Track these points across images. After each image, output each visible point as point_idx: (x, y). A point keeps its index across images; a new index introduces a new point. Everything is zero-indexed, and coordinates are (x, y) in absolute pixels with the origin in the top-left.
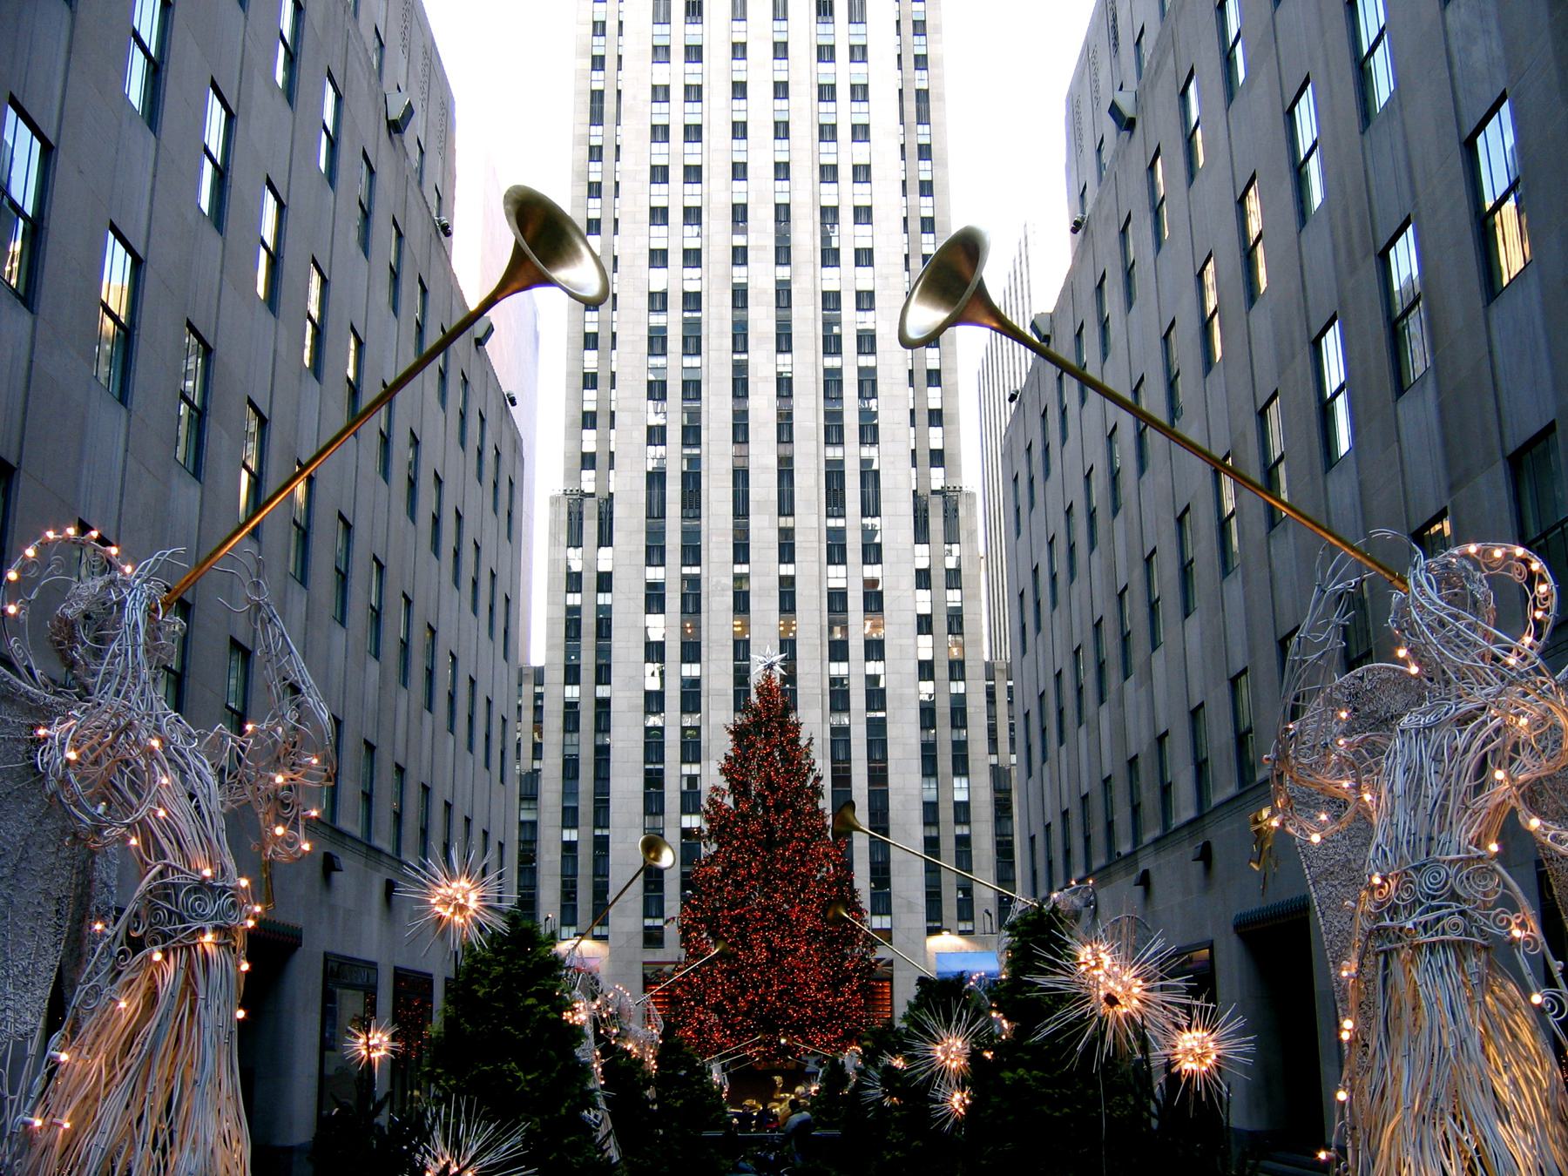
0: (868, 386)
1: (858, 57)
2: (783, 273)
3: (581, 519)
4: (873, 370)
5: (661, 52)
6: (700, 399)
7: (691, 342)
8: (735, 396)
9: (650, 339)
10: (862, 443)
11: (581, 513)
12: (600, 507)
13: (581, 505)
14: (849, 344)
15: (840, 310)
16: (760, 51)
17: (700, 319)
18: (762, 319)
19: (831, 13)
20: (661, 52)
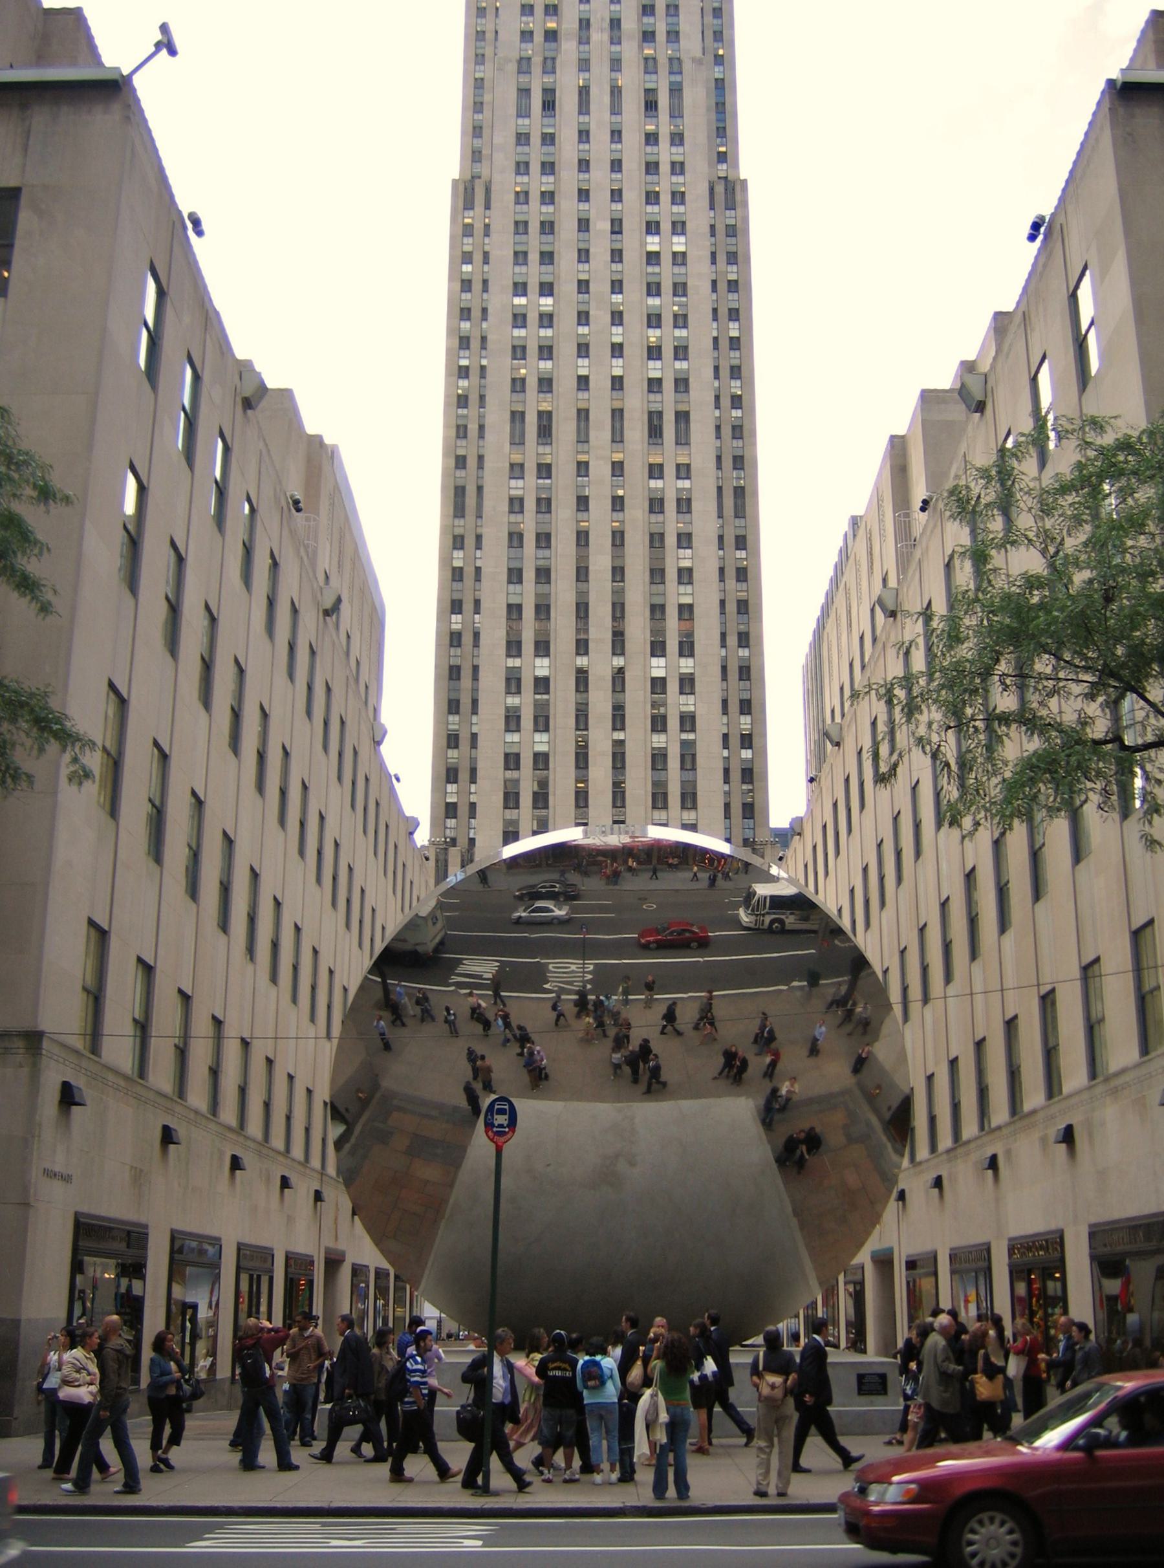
0: (688, 759)
1: (683, 474)
2: (619, 662)
3: (446, 866)
4: (692, 743)
5: (517, 469)
6: (548, 769)
7: (541, 720)
8: (577, 767)
9: (507, 717)
10: (683, 807)
11: (446, 861)
12: (462, 856)
13: (446, 854)
14: (673, 723)
15: (665, 693)
16: (600, 470)
17: (548, 700)
18: (600, 702)
19: (661, 436)
20: (517, 469)
